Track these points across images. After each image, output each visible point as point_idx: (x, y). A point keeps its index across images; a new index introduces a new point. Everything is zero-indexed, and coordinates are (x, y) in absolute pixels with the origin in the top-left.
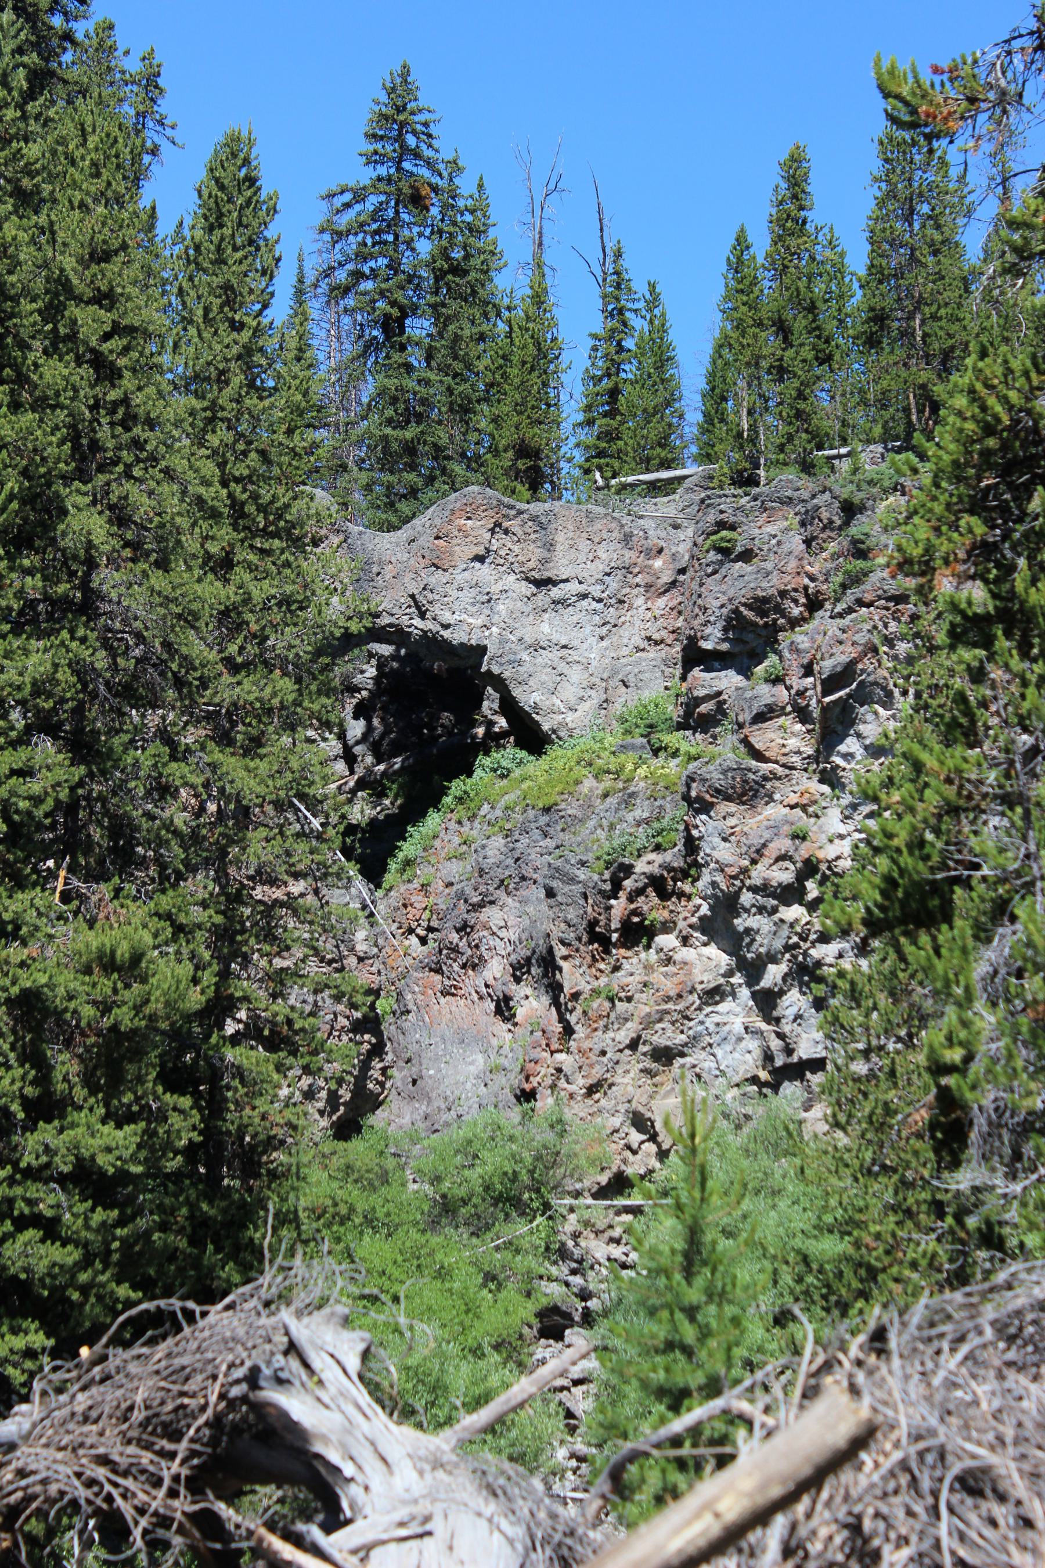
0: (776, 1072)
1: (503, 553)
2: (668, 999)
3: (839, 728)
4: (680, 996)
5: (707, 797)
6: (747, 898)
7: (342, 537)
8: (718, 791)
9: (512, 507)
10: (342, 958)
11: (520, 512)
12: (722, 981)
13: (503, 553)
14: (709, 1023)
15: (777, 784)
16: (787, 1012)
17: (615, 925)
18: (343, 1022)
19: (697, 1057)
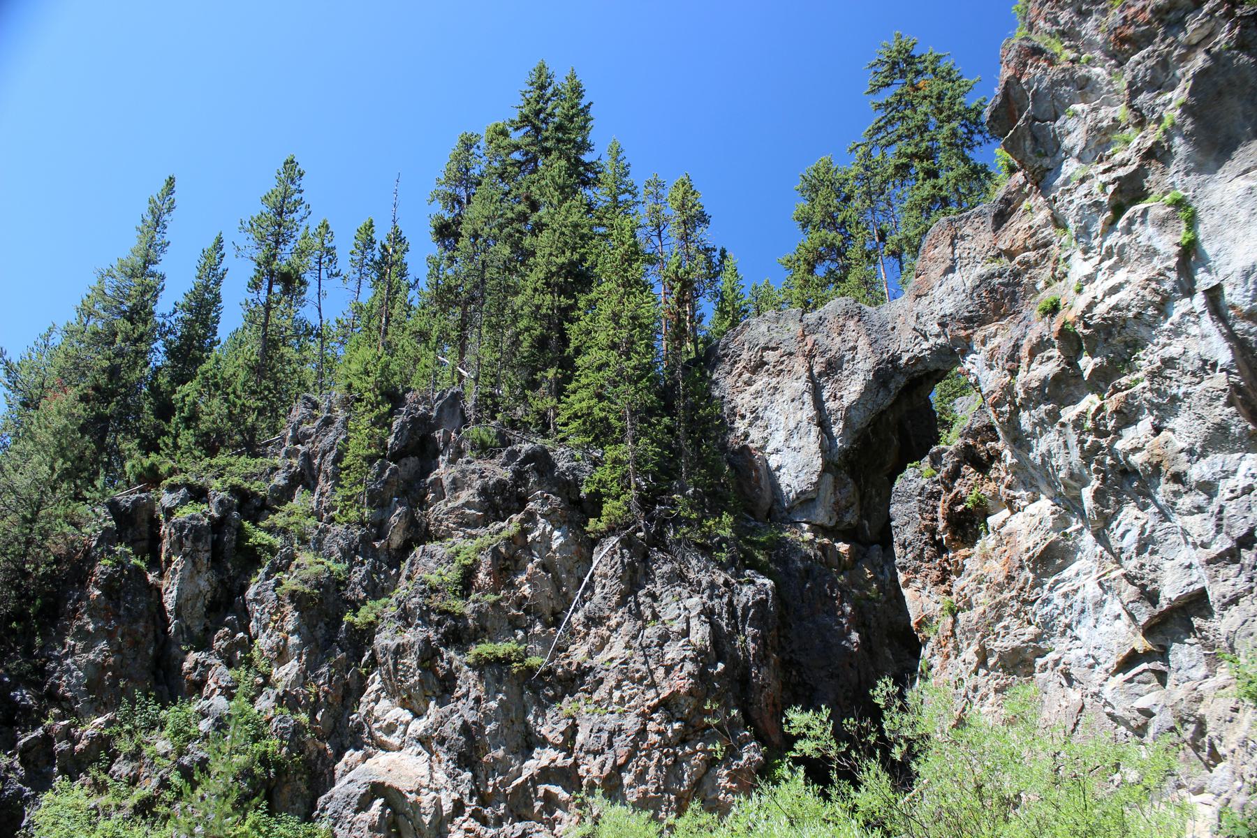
1: (965, 255)
2: (1001, 588)
3: (1047, 162)
4: (1010, 578)
5: (962, 333)
6: (1026, 420)
7: (856, 318)
9: (960, 219)
10: (651, 672)
11: (968, 218)
12: (1054, 536)
13: (965, 255)
14: (1057, 597)
15: (1035, 271)
16: (1124, 544)
17: (941, 525)
19: (1059, 647)
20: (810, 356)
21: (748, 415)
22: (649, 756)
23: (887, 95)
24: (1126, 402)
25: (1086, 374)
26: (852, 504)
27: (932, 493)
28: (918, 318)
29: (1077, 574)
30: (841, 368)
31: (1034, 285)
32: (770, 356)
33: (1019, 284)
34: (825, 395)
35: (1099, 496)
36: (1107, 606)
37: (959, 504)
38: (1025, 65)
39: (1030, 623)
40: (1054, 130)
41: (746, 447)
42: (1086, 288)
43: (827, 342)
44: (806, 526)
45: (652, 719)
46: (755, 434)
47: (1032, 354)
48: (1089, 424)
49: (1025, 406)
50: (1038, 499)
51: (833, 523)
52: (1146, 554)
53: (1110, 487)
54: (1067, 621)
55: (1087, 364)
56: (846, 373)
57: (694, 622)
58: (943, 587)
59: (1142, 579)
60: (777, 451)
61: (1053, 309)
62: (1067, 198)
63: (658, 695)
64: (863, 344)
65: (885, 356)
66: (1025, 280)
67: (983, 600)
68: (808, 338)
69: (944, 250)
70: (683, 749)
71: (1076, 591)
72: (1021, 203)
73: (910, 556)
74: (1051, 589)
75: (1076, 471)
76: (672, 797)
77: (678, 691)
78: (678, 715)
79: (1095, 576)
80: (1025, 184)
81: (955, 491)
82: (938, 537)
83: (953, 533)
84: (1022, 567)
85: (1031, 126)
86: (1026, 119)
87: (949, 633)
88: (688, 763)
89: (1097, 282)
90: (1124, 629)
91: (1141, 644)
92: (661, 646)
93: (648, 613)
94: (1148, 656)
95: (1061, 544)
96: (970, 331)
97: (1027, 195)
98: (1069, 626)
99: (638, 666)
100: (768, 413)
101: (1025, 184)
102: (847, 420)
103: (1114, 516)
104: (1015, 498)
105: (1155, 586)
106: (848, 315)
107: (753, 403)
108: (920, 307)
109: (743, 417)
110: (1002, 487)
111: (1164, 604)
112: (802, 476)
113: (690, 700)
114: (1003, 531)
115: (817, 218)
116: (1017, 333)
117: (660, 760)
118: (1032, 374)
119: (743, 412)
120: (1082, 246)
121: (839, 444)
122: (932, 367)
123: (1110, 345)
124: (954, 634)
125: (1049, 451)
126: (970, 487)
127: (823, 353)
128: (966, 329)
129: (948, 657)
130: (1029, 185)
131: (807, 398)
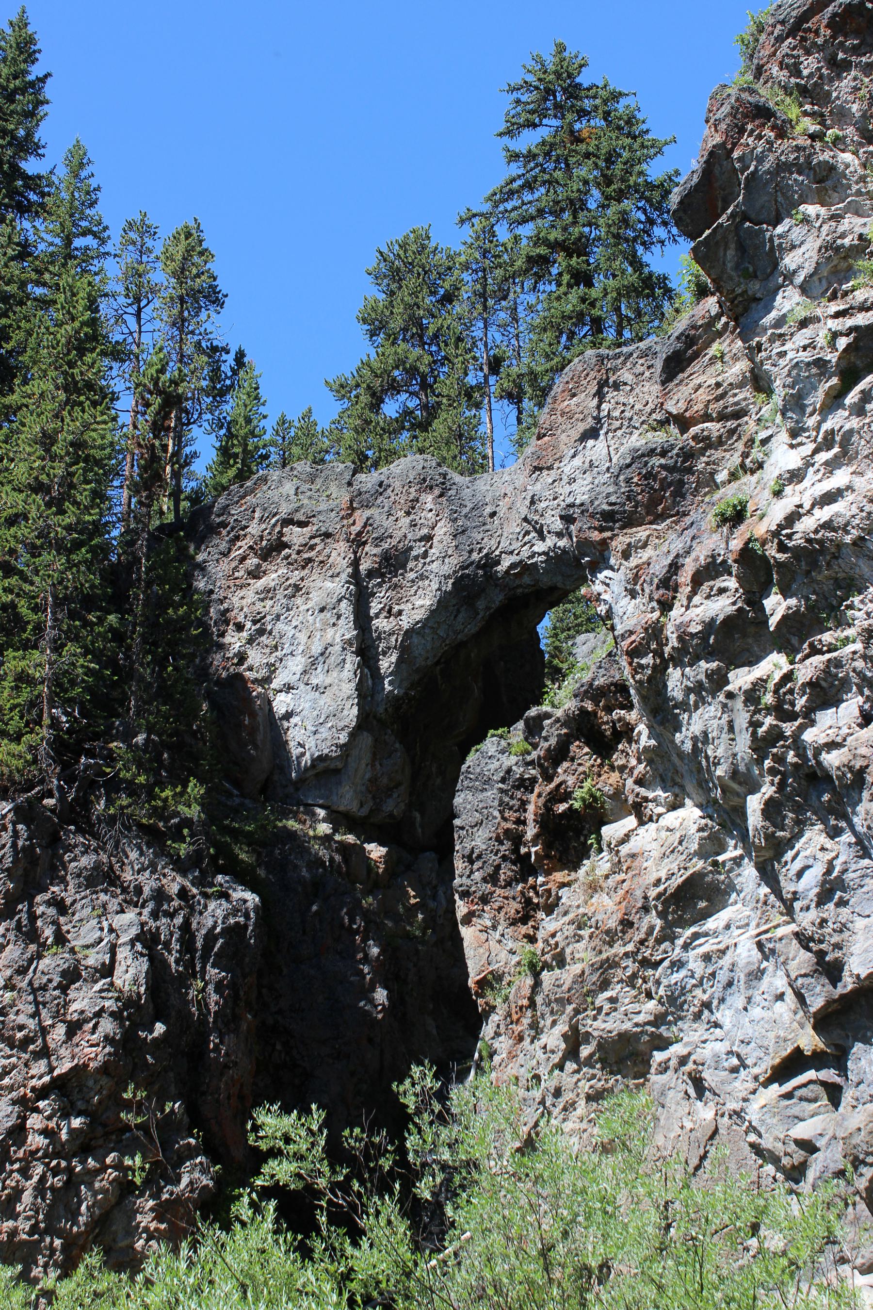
0: (823, 1022)
1: (616, 414)
2: (611, 937)
3: (755, 287)
4: (627, 924)
5: (596, 536)
6: (676, 681)
7: (437, 492)
8: (609, 517)
9: (617, 356)
10: (44, 1031)
12: (699, 865)
13: (616, 414)
15: (717, 454)
17: (531, 831)
18: (36, 1141)
19: (690, 1037)
20: (357, 542)
21: (248, 625)
22: (25, 1173)
23: (529, 140)
24: (826, 671)
25: (773, 622)
26: (397, 786)
27: (522, 780)
28: (532, 502)
29: (728, 927)
30: (404, 566)
31: (712, 474)
32: (295, 535)
33: (690, 471)
34: (375, 607)
35: (771, 809)
36: (766, 979)
37: (561, 801)
38: (742, 131)
39: (649, 996)
40: (771, 239)
41: (239, 677)
42: (788, 490)
43: (386, 524)
44: (321, 813)
45: (37, 1110)
46: (255, 657)
47: (697, 581)
48: (768, 699)
49: (677, 659)
50: (682, 805)
51: (364, 812)
52: (831, 906)
53: (790, 798)
54: (705, 997)
55: (777, 606)
56: (411, 575)
57: (123, 953)
58: (523, 929)
59: (821, 942)
60: (288, 688)
61: (736, 516)
62: (777, 348)
63: (51, 1069)
64: (442, 530)
65: (475, 556)
66: (700, 467)
67: (583, 955)
68: (357, 513)
69: (586, 402)
70: (83, 1162)
71: (723, 952)
72: (708, 345)
73: (477, 876)
74: (686, 947)
75: (742, 768)
76: (58, 1242)
77: (86, 1066)
78: (80, 1105)
79: (753, 931)
80: (718, 316)
81: (557, 781)
82: (523, 850)
83: (547, 846)
84: (646, 909)
85: (738, 227)
86: (733, 216)
87: (525, 1002)
88: (90, 1186)
89: (806, 483)
90: (787, 1016)
91: (809, 1040)
92: (64, 989)
93: (48, 932)
94: (818, 1060)
95: (709, 879)
96: (608, 534)
97: (720, 334)
98: (707, 1005)
99: (22, 1019)
100: (280, 626)
101: (718, 316)
102: (404, 650)
103: (789, 843)
104: (646, 799)
105: (838, 954)
106: (425, 484)
107: (259, 606)
108: (538, 486)
109: (240, 627)
110: (630, 782)
111: (847, 984)
112: (324, 732)
113: (104, 1081)
114: (624, 850)
115: (396, 324)
116: (677, 545)
117: (43, 1179)
118: (693, 613)
119: (240, 619)
120: (790, 424)
121: (388, 687)
122: (546, 581)
123: (813, 581)
124: (532, 1004)
125: (705, 734)
126: (582, 777)
127: (381, 539)
128: (601, 530)
129: (521, 1039)
130: (724, 319)
131: (346, 608)
